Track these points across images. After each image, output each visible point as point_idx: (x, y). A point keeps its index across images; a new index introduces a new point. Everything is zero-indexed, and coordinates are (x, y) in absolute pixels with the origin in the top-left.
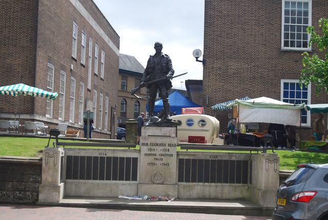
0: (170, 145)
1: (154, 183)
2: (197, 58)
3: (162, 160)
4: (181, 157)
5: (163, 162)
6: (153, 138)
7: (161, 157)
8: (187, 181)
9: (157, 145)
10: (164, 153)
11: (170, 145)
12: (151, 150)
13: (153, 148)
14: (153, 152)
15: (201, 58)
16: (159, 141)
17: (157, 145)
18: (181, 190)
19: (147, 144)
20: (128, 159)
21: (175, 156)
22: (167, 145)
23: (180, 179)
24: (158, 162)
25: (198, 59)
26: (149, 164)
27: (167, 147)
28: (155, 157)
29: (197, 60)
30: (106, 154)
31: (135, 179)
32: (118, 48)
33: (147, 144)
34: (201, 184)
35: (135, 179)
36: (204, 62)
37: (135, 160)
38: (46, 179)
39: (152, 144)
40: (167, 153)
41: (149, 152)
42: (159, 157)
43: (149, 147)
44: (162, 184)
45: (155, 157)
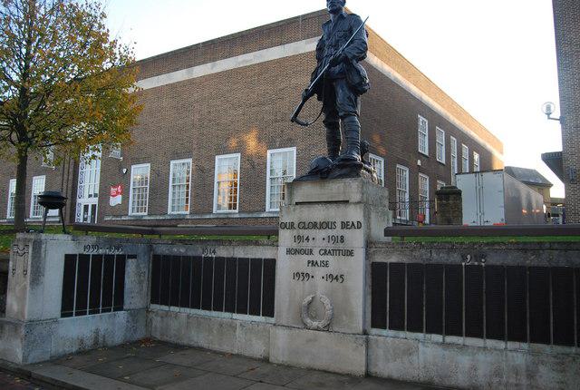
0: (345, 225)
1: (306, 327)
2: (548, 114)
3: (326, 264)
4: (379, 259)
5: (331, 270)
6: (305, 209)
7: (325, 258)
8: (397, 326)
9: (314, 225)
10: (330, 246)
11: (345, 225)
12: (299, 238)
13: (305, 233)
14: (305, 245)
15: (557, 113)
16: (318, 214)
17: (314, 225)
18: (379, 352)
19: (292, 226)
20: (256, 262)
21: (360, 254)
22: (339, 225)
23: (378, 320)
24: (320, 272)
25: (551, 116)
26: (297, 275)
27: (338, 232)
28: (310, 258)
29: (549, 118)
30: (214, 252)
31: (269, 312)
32: (502, 153)
33: (292, 226)
34: (438, 338)
35: (269, 312)
36: (562, 120)
37: (271, 265)
38: (12, 305)
39: (303, 225)
40: (341, 246)
41: (295, 246)
42: (317, 257)
43: (295, 233)
44: (327, 328)
45: (310, 258)
